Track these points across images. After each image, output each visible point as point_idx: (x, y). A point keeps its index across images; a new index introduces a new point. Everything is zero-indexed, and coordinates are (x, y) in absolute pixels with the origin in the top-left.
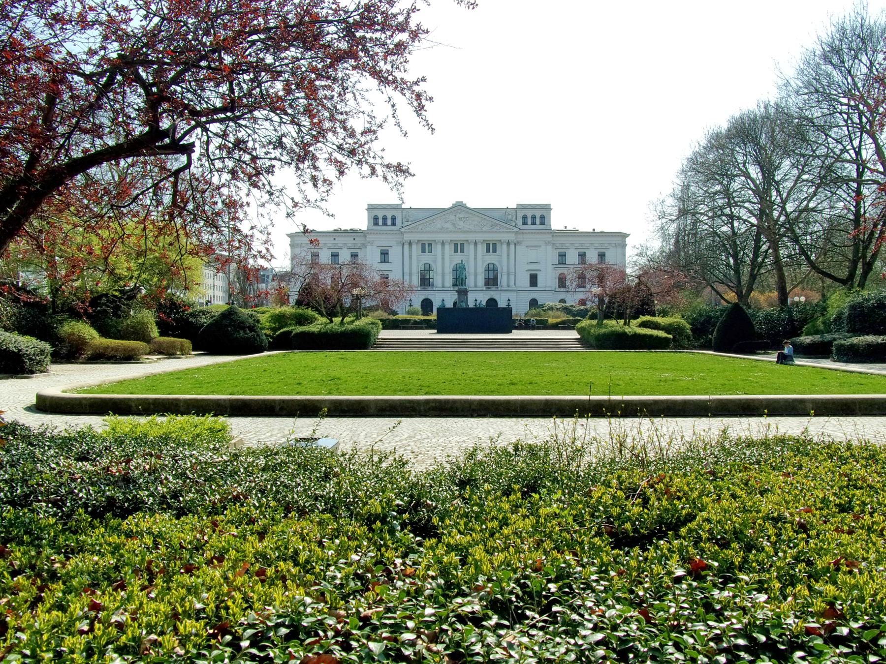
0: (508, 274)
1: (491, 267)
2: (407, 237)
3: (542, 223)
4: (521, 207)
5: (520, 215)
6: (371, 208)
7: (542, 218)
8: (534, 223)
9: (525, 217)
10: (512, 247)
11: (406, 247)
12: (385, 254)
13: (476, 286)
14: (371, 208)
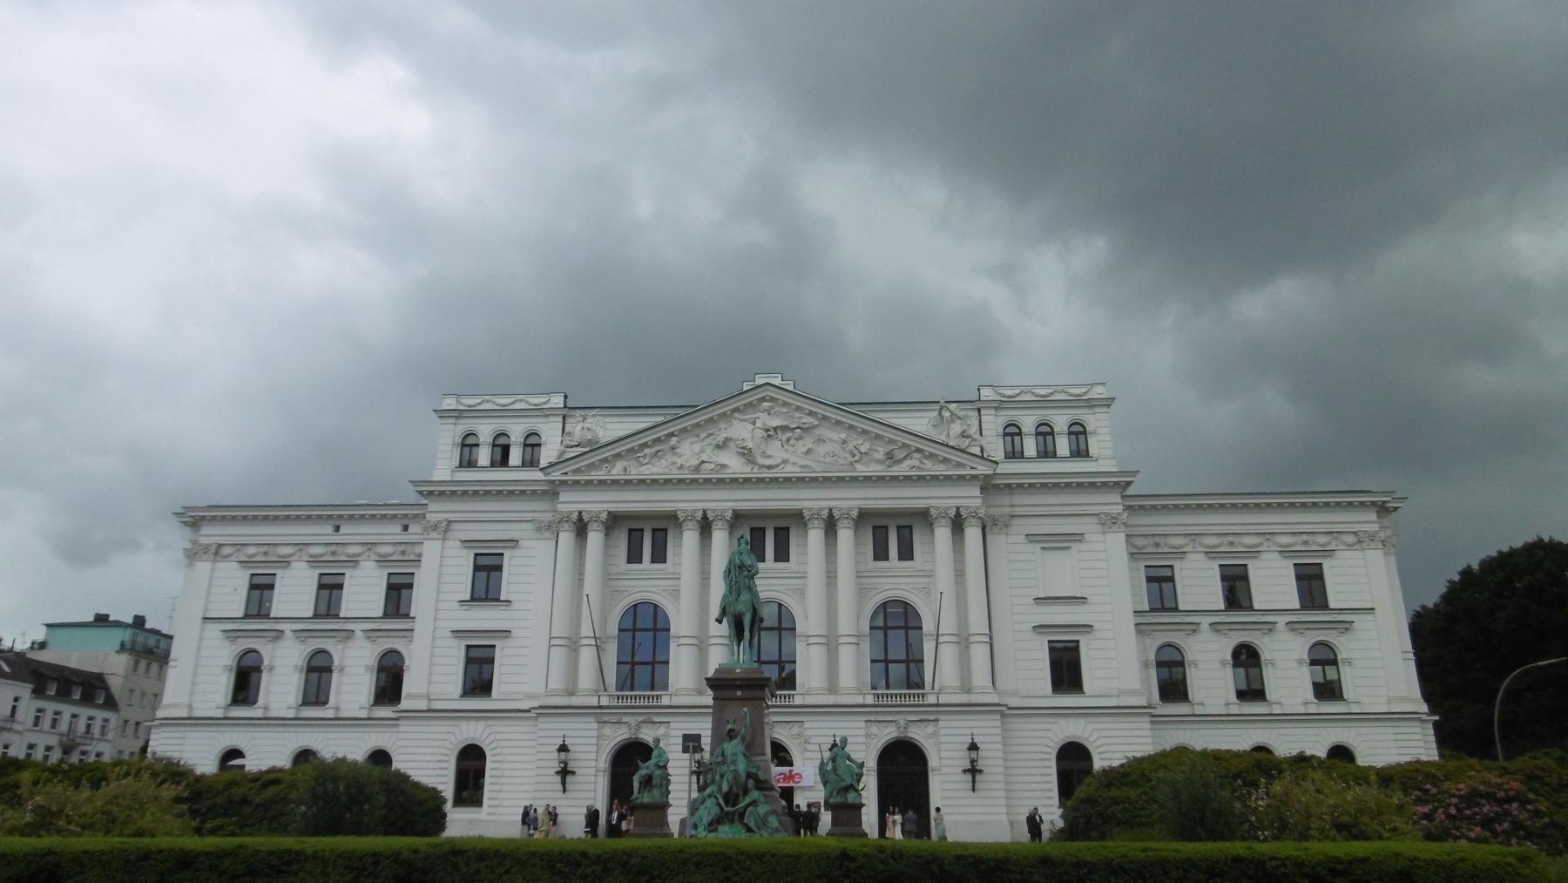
0: (964, 642)
2: (571, 502)
3: (1080, 452)
5: (993, 423)
7: (1078, 432)
8: (1047, 453)
9: (1012, 432)
10: (972, 534)
11: (567, 538)
12: (487, 575)
13: (832, 688)
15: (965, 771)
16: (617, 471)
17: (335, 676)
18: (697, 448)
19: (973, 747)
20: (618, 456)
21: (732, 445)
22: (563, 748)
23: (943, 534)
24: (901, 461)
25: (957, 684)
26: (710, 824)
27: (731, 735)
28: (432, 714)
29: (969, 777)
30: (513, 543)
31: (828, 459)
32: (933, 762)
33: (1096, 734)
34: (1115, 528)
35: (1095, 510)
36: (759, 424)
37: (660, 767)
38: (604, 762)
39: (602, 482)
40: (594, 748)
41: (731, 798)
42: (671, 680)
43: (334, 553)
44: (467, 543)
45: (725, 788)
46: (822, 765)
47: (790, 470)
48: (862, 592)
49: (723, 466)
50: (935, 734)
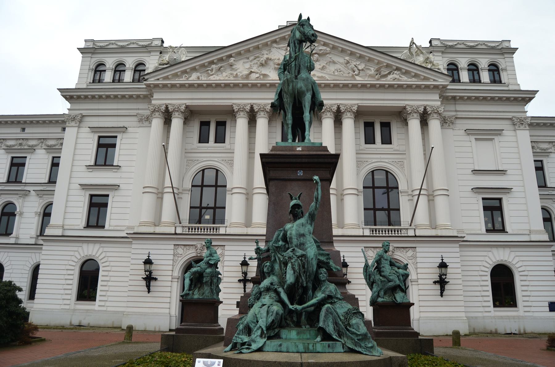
1: (380, 179)
2: (161, 99)
4: (447, 47)
6: (90, 50)
7: (494, 69)
10: (434, 124)
11: (157, 123)
14: (90, 50)
15: (435, 282)
16: (193, 78)
17: (17, 218)
18: (247, 66)
19: (443, 265)
20: (194, 69)
21: (271, 63)
22: (148, 262)
23: (414, 124)
24: (385, 76)
25: (427, 222)
26: (269, 328)
27: (296, 213)
28: (63, 239)
29: (438, 287)
30: (124, 129)
31: (336, 73)
32: (413, 276)
33: (517, 259)
34: (522, 127)
35: (510, 115)
37: (210, 266)
38: (177, 273)
39: (182, 86)
40: (171, 262)
41: (297, 292)
42: (226, 217)
43: (21, 144)
44: (93, 129)
45: (290, 278)
46: (366, 267)
48: (359, 163)
49: (265, 75)
50: (414, 257)
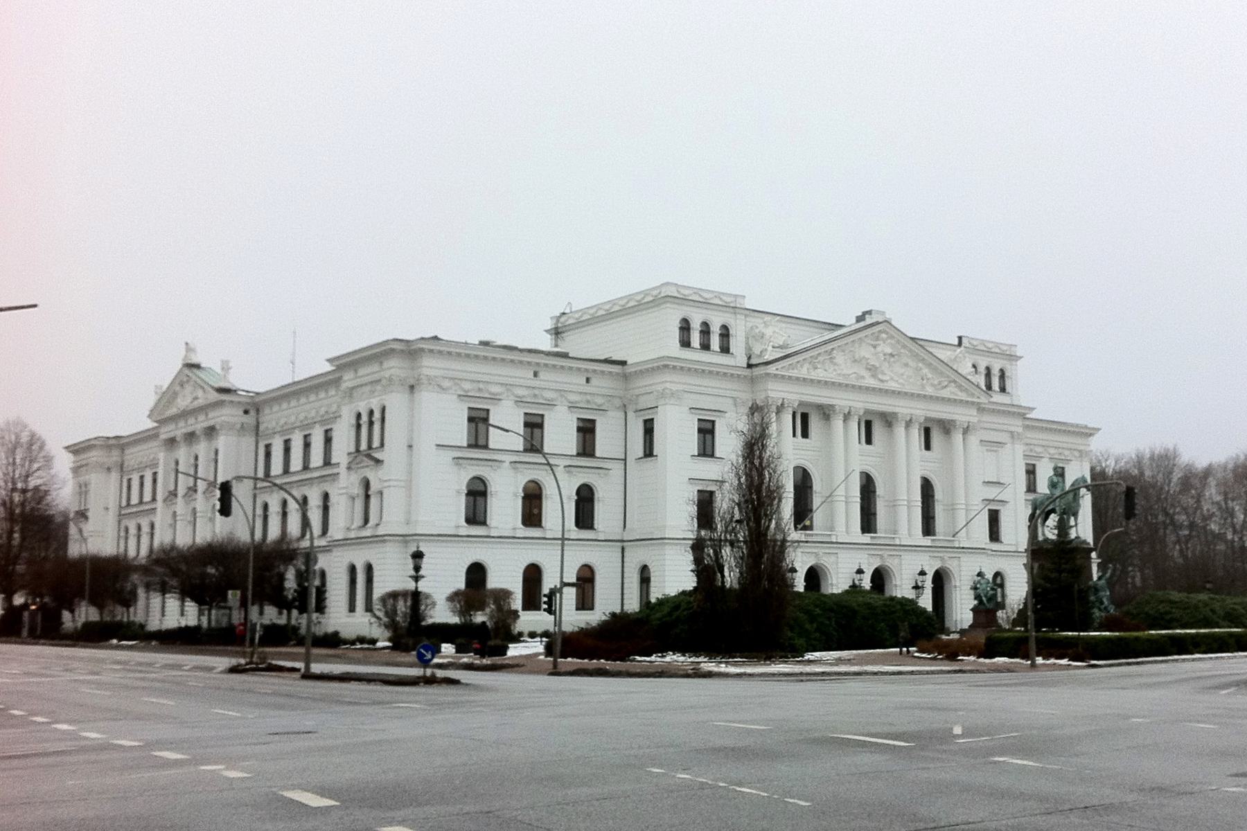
16: (804, 372)
36: (879, 349)
47: (893, 385)
49: (863, 377)
